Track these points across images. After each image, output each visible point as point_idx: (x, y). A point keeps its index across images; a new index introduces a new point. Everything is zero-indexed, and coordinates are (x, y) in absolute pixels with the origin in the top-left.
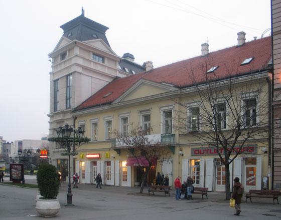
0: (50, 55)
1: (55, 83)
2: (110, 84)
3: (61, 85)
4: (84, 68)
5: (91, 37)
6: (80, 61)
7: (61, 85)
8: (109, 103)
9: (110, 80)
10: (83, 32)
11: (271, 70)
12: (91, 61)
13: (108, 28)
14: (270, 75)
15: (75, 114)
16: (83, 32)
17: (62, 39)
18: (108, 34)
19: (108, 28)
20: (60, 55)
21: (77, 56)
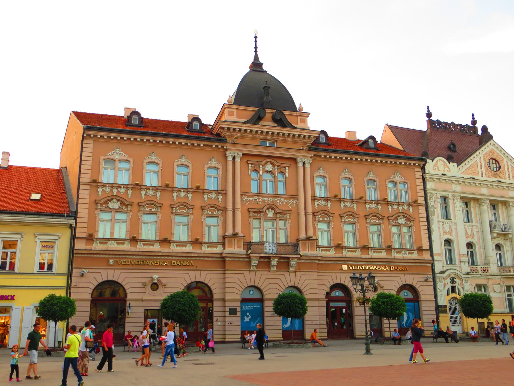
11: (76, 218)
14: (72, 221)
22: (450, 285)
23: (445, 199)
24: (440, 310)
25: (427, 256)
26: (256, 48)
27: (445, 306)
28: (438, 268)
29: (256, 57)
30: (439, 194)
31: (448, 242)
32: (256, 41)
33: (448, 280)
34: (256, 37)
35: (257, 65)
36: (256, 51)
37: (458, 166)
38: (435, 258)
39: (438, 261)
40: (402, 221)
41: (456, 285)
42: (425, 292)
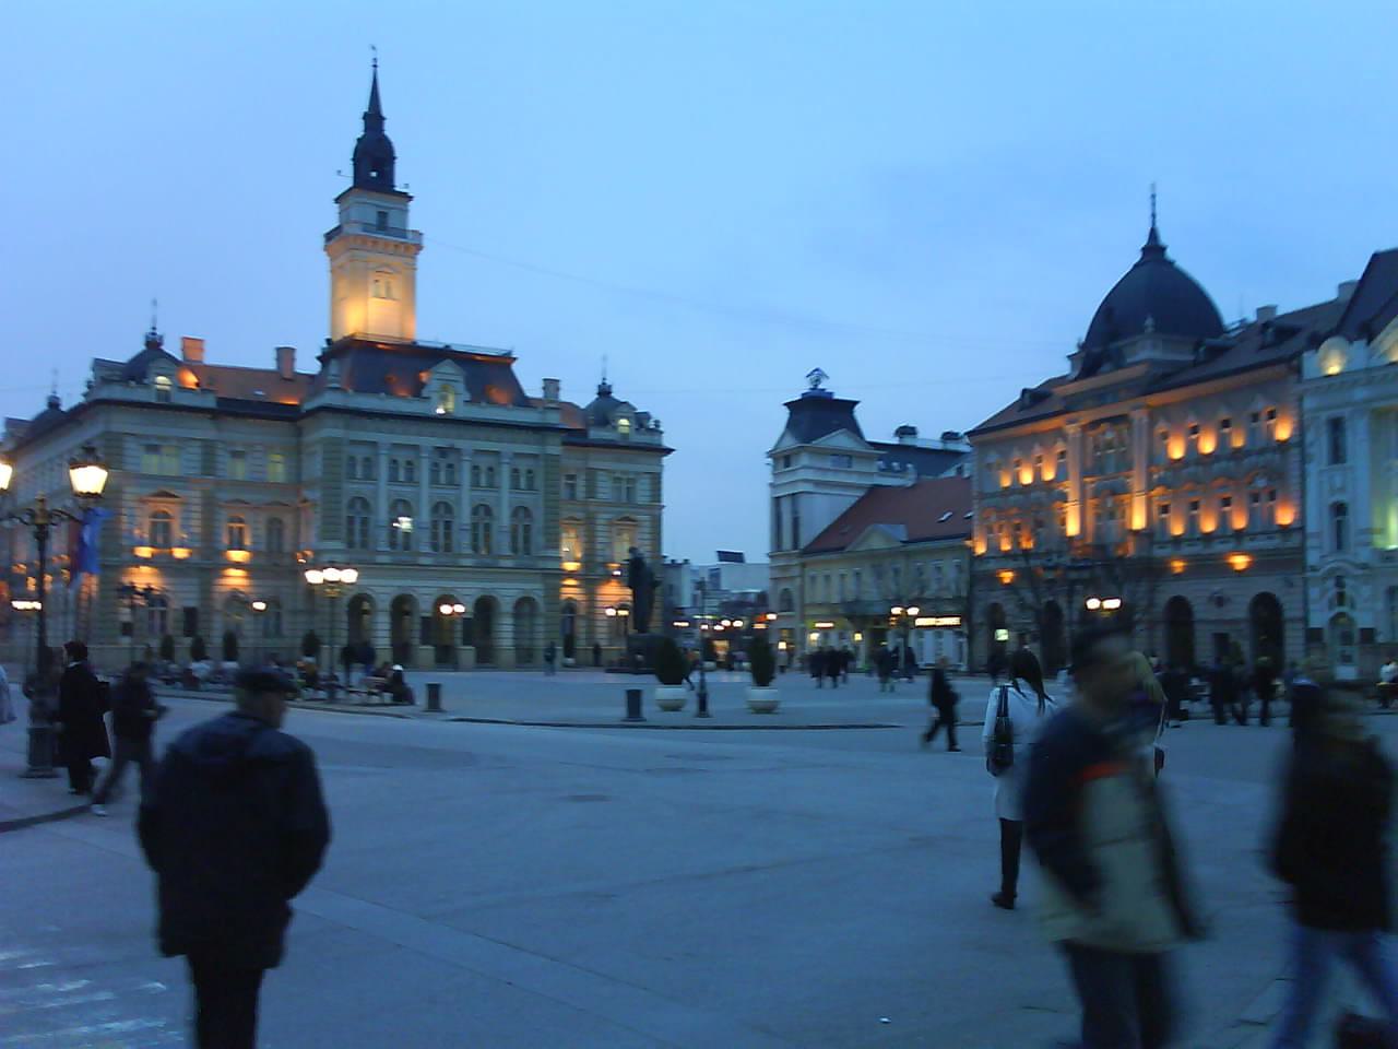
0: (771, 454)
1: (777, 501)
2: (861, 500)
3: (786, 507)
4: (817, 483)
5: (829, 429)
6: (810, 475)
7: (786, 507)
8: (841, 549)
9: (860, 493)
10: (819, 414)
12: (829, 470)
13: (856, 403)
14: (968, 543)
15: (804, 560)
16: (819, 414)
17: (782, 437)
18: (858, 412)
19: (856, 403)
20: (782, 459)
21: (804, 467)
22: (1333, 592)
23: (1336, 426)
24: (1313, 636)
25: (1295, 541)
26: (1154, 216)
27: (1319, 630)
28: (1312, 558)
29: (1153, 234)
30: (1324, 416)
31: (1340, 509)
32: (1154, 204)
33: (1331, 583)
34: (1153, 196)
35: (1154, 250)
36: (1154, 223)
37: (1369, 343)
38: (1310, 542)
39: (1313, 548)
40: (1261, 483)
41: (1348, 591)
42: (1291, 610)
